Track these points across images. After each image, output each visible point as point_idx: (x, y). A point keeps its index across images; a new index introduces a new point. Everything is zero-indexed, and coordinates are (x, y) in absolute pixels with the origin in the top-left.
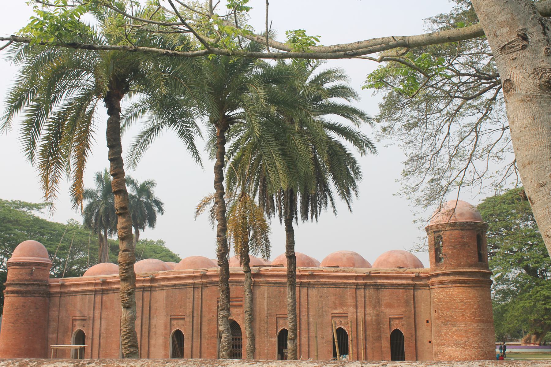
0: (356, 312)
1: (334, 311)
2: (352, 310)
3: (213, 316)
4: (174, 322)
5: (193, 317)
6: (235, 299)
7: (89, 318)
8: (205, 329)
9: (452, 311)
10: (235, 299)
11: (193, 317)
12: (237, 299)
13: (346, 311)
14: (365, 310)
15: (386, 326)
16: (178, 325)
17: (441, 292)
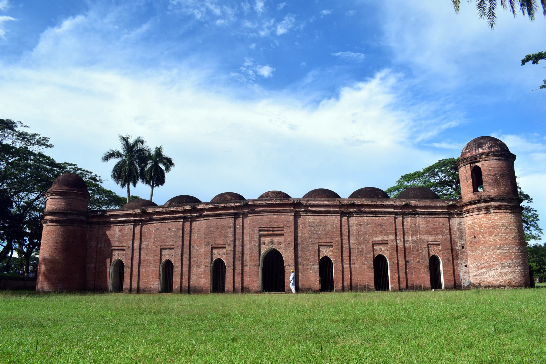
0: (396, 240)
1: (375, 239)
2: (392, 237)
3: (255, 245)
4: (215, 251)
5: (234, 246)
6: (276, 229)
7: (129, 247)
8: (247, 258)
9: (496, 235)
10: (276, 229)
11: (234, 246)
12: (278, 228)
13: (386, 239)
14: (404, 238)
15: (425, 252)
16: (219, 254)
17: (482, 218)
